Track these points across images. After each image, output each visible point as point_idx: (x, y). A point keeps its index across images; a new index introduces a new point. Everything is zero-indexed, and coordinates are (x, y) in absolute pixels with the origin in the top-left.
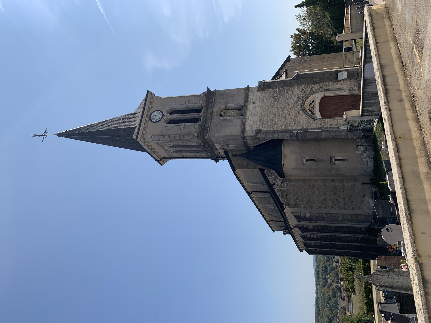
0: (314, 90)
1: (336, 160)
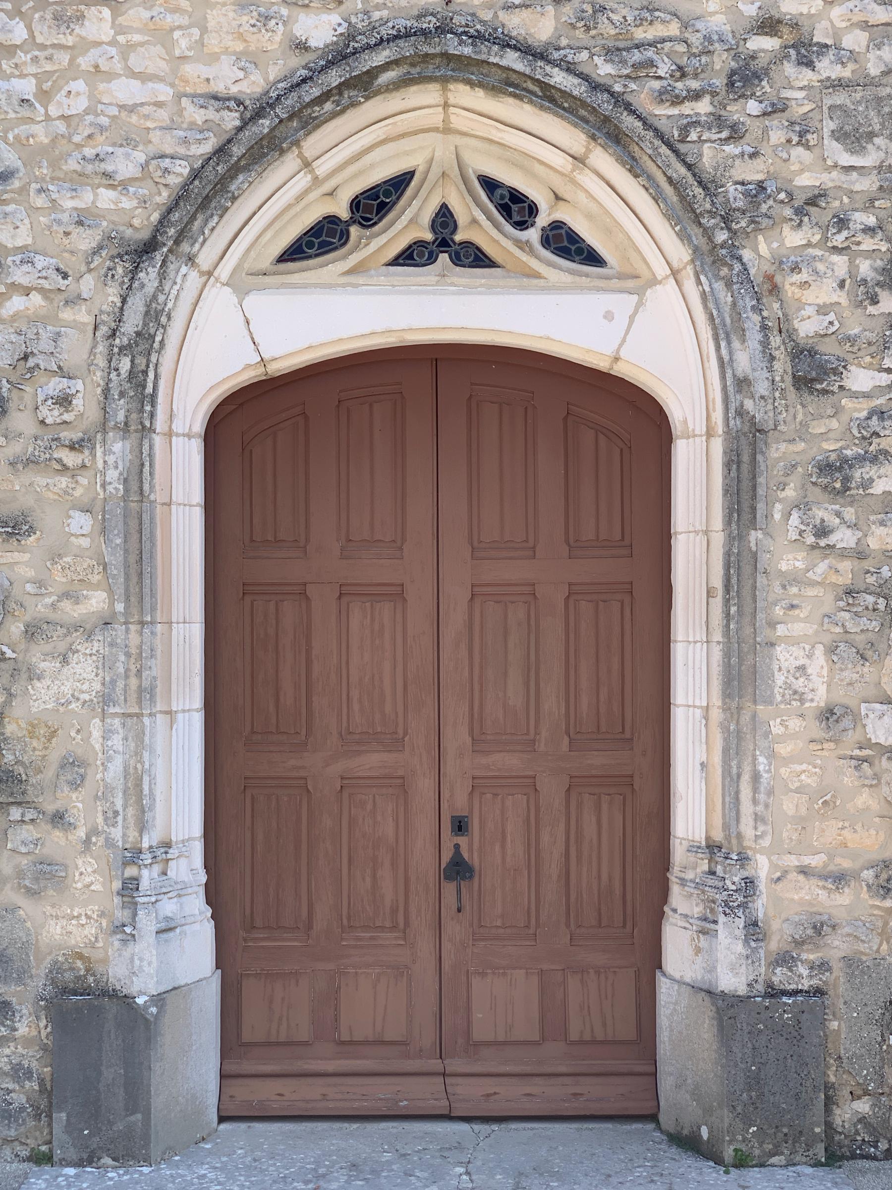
0: (759, 252)
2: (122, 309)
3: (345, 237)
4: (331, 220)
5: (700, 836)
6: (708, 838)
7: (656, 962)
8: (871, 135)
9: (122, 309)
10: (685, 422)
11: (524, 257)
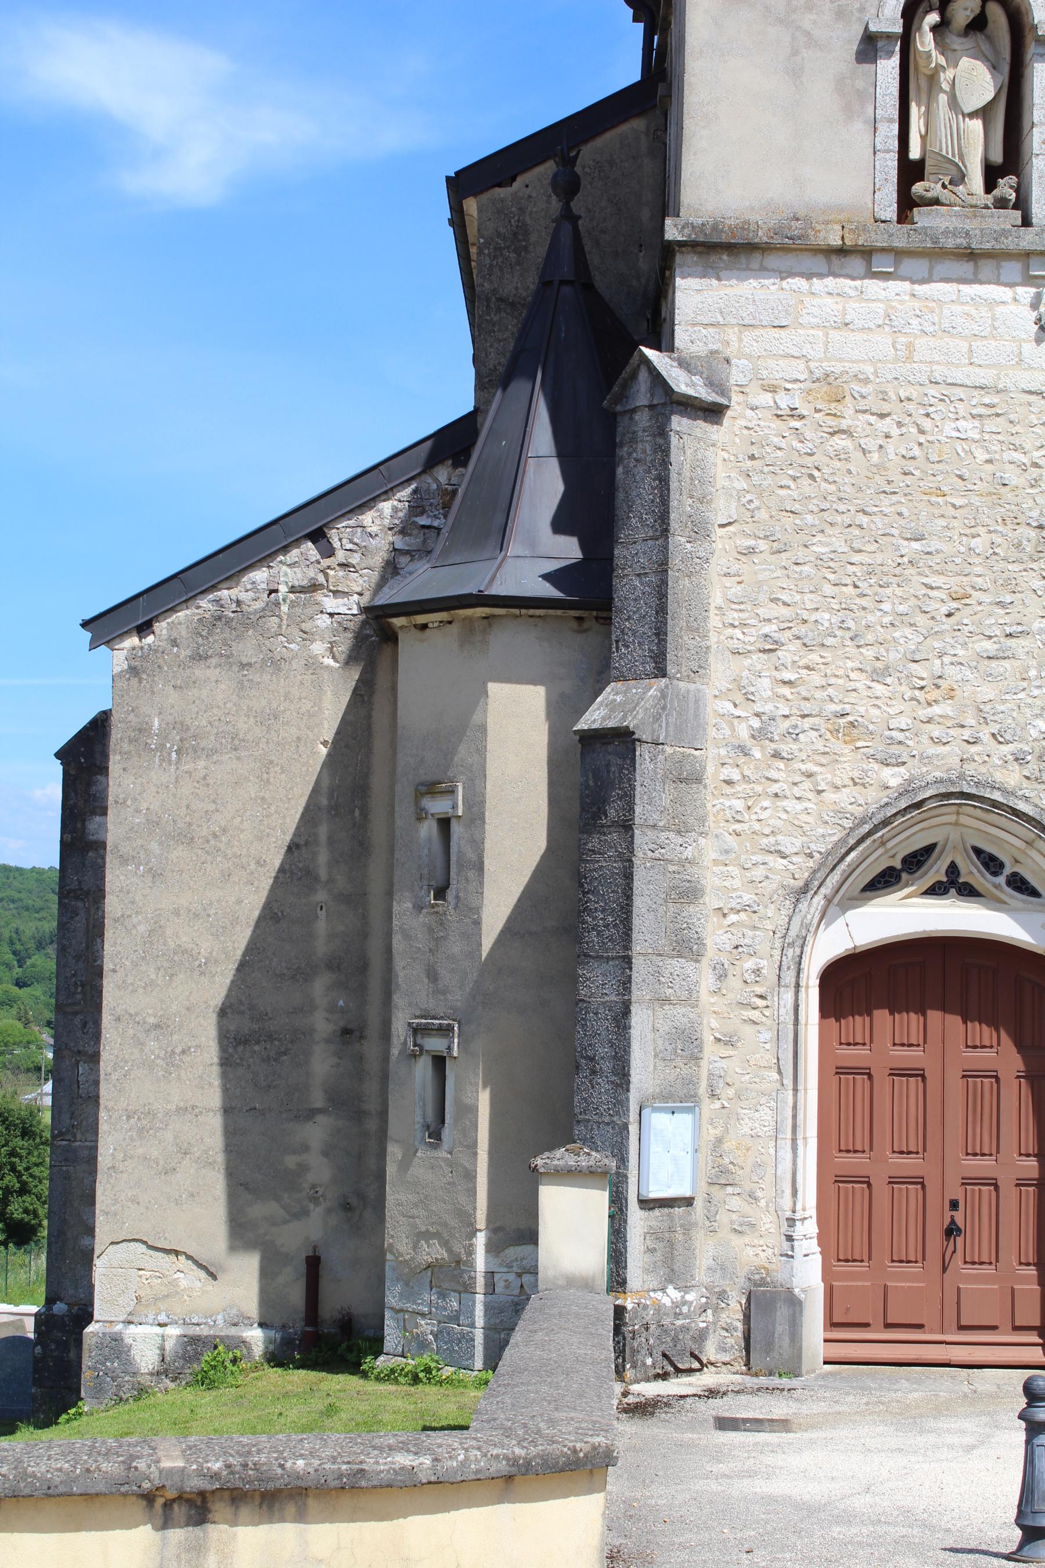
1: (439, 1062)
2: (789, 923)
4: (891, 869)
9: (789, 923)
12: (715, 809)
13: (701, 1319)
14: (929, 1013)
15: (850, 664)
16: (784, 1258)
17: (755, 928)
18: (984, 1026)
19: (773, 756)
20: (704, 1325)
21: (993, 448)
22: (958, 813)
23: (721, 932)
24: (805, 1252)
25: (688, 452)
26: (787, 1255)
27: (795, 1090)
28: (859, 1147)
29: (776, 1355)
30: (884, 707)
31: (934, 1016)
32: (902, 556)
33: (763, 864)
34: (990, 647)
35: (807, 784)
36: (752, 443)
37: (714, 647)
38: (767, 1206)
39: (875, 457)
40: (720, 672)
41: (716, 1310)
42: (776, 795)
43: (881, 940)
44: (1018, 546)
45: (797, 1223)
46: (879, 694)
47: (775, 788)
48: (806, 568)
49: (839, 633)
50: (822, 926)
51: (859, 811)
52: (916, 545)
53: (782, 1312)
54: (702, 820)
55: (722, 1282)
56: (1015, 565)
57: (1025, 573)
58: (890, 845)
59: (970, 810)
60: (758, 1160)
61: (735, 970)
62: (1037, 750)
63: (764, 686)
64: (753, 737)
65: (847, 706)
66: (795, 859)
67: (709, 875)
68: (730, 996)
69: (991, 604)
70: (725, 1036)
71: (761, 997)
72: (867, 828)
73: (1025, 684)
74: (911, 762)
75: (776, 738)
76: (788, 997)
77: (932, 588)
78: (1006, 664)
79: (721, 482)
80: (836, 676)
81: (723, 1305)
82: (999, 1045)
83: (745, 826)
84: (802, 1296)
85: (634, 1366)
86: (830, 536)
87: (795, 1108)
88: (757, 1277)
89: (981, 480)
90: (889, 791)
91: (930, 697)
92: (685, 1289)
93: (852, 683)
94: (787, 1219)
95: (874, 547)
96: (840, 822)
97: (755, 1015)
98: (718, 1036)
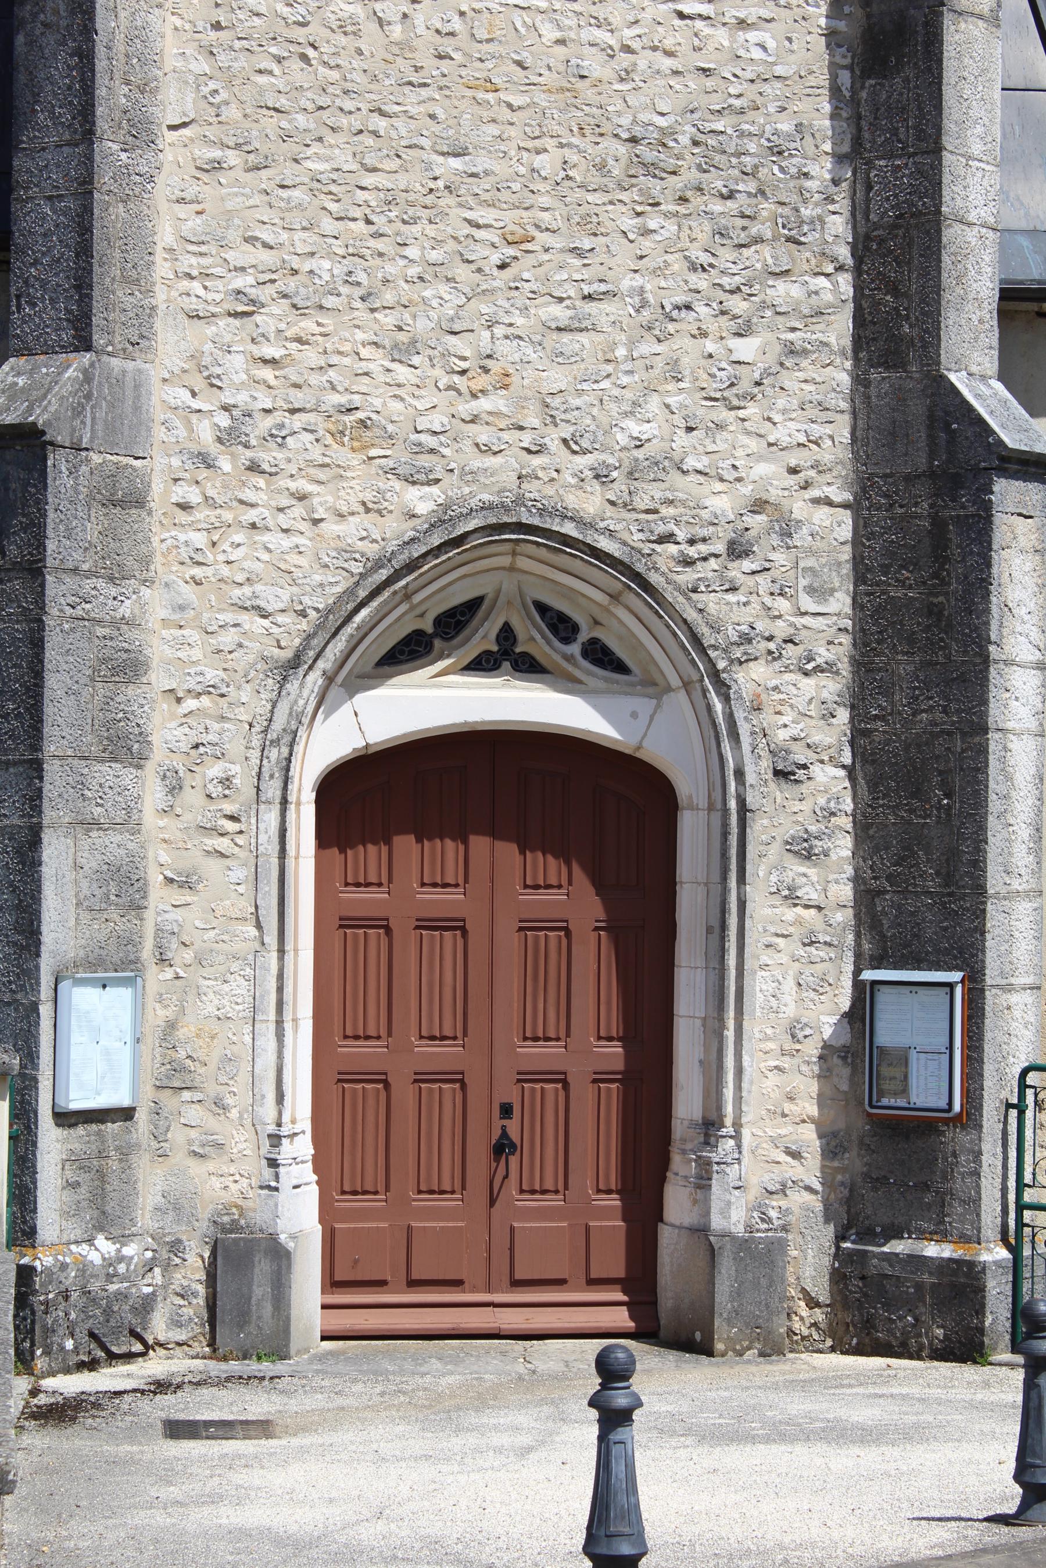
2: (272, 712)
3: (429, 648)
4: (419, 633)
5: (697, 1115)
6: (703, 1118)
7: (658, 1215)
8: (832, 591)
9: (272, 712)
10: (691, 797)
11: (570, 668)
12: (164, 546)
13: (145, 1281)
14: (473, 839)
15: (360, 336)
16: (266, 1192)
17: (223, 718)
18: (550, 858)
19: (249, 469)
20: (150, 1289)
21: (567, 22)
22: (514, 554)
23: (174, 724)
24: (295, 1182)
25: (122, 14)
26: (269, 1187)
27: (281, 951)
28: (372, 1032)
29: (252, 1328)
30: (409, 400)
31: (479, 844)
32: (435, 179)
33: (235, 625)
34: (559, 313)
35: (299, 510)
36: (217, 5)
37: (162, 307)
38: (241, 1117)
39: (397, 31)
40: (172, 344)
41: (167, 1267)
42: (254, 526)
43: (404, 735)
44: (601, 167)
45: (284, 1140)
46: (401, 379)
47: (251, 515)
48: (296, 193)
49: (344, 290)
50: (320, 716)
51: (372, 550)
52: (455, 163)
53: (262, 1268)
54: (145, 562)
55: (176, 1228)
56: (597, 195)
57: (610, 207)
58: (417, 598)
59: (531, 549)
60: (228, 1052)
61: (194, 779)
62: (626, 463)
63: (236, 366)
64: (220, 440)
65: (356, 397)
66: (280, 619)
67: (155, 641)
68: (187, 817)
69: (562, 251)
70: (180, 874)
71: (233, 818)
72: (384, 574)
73: (609, 368)
74: (447, 480)
75: (254, 442)
76: (271, 818)
77: (478, 226)
78: (584, 338)
79: (171, 62)
80: (340, 353)
81: (177, 1261)
82: (570, 883)
83: (209, 571)
84: (291, 1245)
85: (47, 1353)
86: (331, 146)
87: (280, 976)
88: (226, 1219)
89: (549, 68)
90: (416, 522)
91: (477, 385)
92: (123, 1239)
93: (363, 364)
94: (269, 1136)
95: (394, 164)
96: (346, 565)
97: (223, 844)
98: (170, 875)
